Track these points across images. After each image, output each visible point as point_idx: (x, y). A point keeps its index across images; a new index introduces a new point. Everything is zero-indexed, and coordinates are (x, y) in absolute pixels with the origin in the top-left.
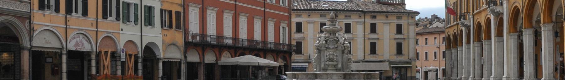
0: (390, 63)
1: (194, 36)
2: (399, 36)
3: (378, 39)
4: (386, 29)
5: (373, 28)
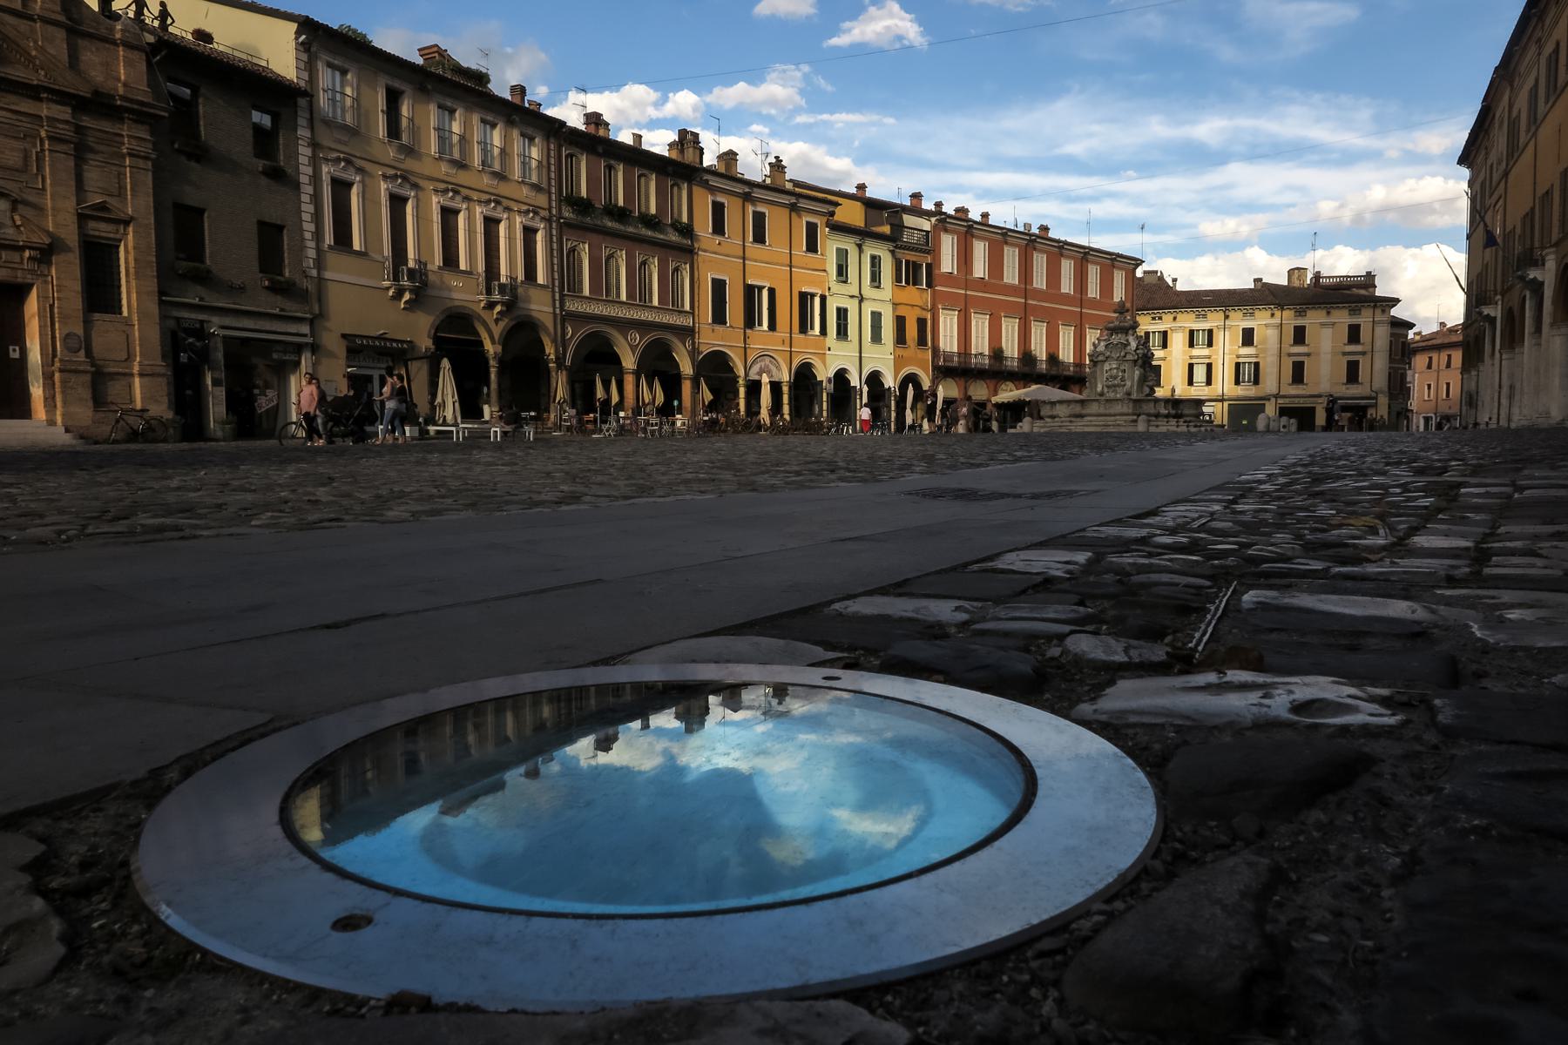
1: (948, 356)
3: (1308, 355)
4: (1327, 332)
5: (1300, 335)
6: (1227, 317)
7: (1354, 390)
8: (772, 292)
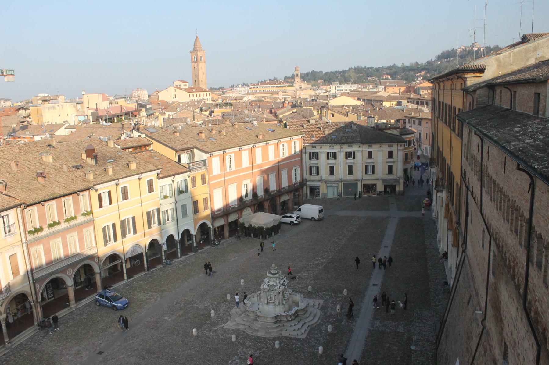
0: (384, 181)
2: (390, 160)
4: (380, 154)
5: (370, 155)
6: (341, 147)
7: (391, 177)
8: (134, 219)
